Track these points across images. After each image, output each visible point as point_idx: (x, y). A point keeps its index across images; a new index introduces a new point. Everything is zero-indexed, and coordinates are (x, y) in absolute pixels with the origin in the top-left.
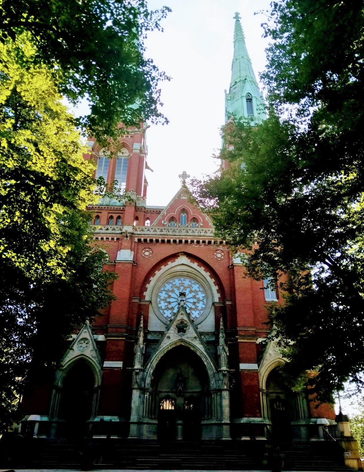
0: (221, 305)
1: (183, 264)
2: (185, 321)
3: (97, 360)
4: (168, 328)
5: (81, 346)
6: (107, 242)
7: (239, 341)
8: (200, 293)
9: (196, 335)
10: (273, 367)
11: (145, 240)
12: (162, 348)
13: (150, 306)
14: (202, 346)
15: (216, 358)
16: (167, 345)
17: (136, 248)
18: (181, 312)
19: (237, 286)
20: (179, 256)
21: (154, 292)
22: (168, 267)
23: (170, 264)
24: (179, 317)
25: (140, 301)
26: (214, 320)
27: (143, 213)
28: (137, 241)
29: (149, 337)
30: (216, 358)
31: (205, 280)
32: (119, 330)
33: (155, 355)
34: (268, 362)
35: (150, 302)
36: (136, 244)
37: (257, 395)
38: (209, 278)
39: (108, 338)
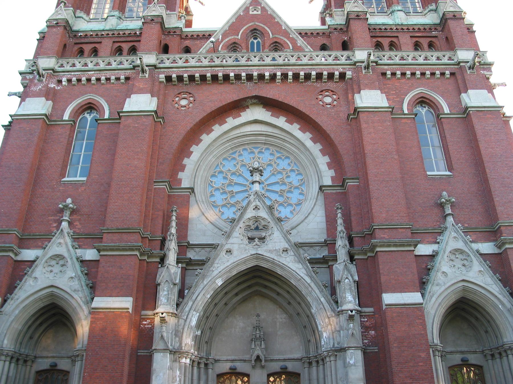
0: (339, 190)
1: (256, 122)
2: (264, 219)
3: (81, 295)
4: (228, 235)
5: (51, 271)
6: (108, 86)
7: (378, 249)
8: (293, 175)
9: (287, 246)
10: (453, 299)
11: (180, 78)
12: (216, 273)
13: (192, 199)
14: (300, 266)
15: (332, 290)
16: (226, 265)
17: (162, 92)
18: (254, 204)
19: (368, 148)
20: (248, 107)
21: (201, 173)
22: (226, 127)
23: (231, 122)
24: (250, 213)
25: (171, 188)
26: (324, 219)
27: (178, 38)
28: (164, 80)
29: (191, 255)
30: (332, 290)
31: (302, 149)
32: (125, 236)
33: (202, 286)
34: (443, 288)
35: (192, 190)
36: (162, 86)
37: (423, 355)
38: (309, 144)
39: (102, 253)
